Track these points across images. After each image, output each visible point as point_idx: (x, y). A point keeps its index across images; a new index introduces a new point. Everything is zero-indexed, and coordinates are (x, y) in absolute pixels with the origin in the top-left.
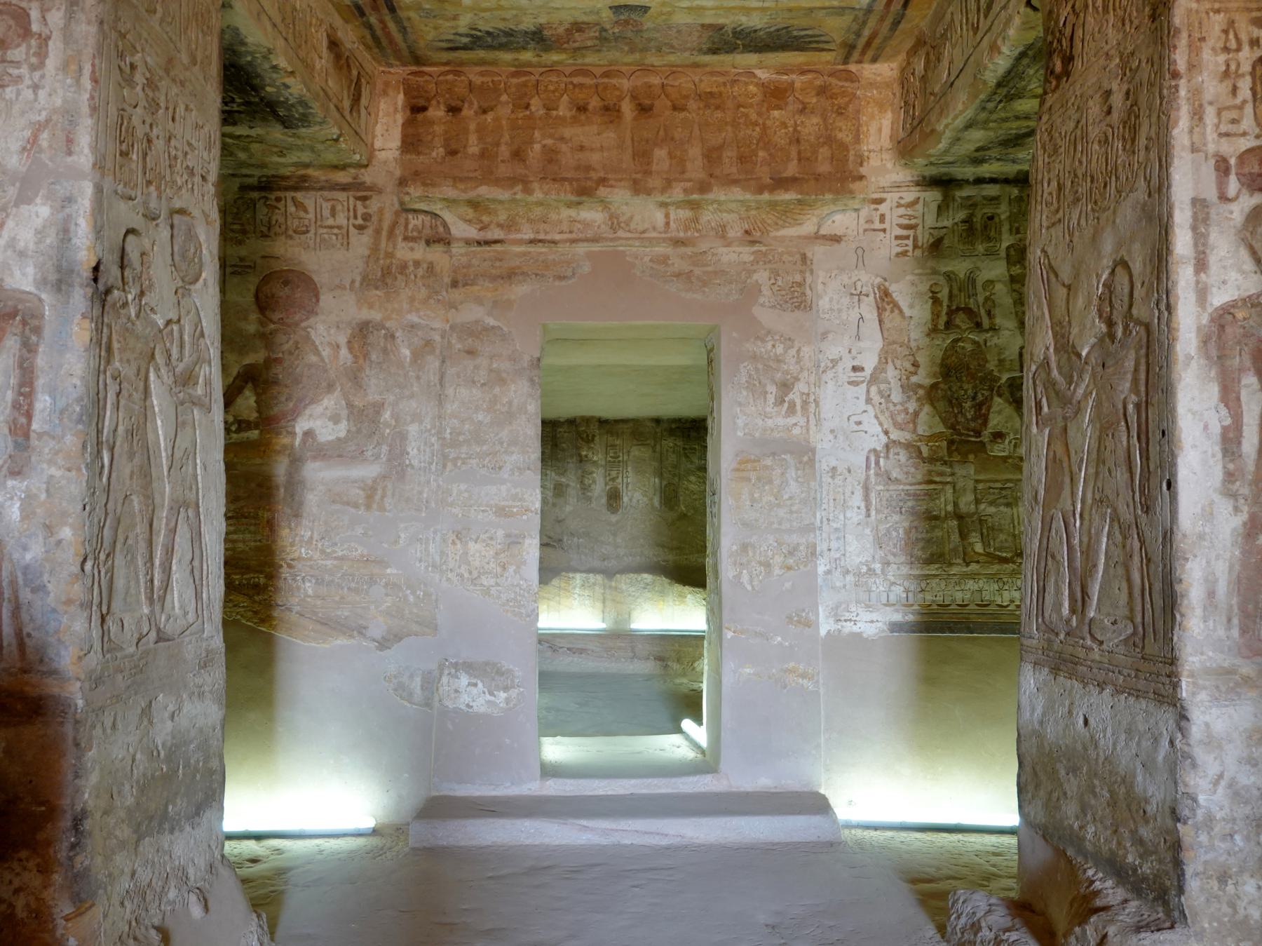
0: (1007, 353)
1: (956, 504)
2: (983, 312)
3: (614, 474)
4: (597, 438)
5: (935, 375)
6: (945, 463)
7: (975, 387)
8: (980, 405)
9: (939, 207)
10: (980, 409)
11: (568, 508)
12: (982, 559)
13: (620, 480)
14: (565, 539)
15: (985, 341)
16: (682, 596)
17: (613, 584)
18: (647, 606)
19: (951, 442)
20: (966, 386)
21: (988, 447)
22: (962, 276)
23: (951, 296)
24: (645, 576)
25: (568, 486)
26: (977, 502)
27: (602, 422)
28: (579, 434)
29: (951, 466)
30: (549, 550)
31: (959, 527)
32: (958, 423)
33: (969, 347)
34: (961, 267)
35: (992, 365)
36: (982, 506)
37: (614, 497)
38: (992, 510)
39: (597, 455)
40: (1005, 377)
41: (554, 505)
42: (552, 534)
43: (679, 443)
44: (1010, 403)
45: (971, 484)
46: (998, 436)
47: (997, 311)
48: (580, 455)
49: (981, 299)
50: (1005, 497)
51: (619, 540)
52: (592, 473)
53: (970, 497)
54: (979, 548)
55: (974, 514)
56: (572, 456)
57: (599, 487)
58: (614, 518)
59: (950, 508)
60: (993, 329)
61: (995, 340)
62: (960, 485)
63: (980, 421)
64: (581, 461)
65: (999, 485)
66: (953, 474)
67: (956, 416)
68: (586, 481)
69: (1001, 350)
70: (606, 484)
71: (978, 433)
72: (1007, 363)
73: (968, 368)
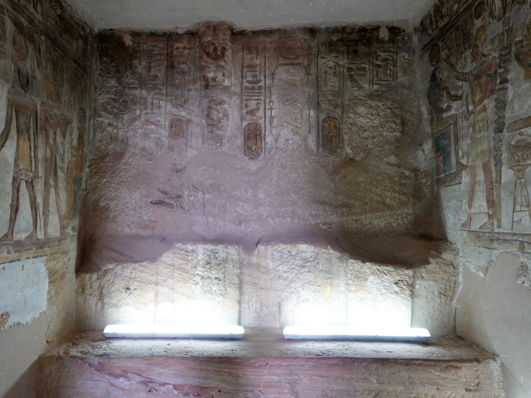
3: (252, 104)
4: (228, 53)
11: (191, 153)
13: (261, 113)
14: (186, 193)
16: (361, 278)
17: (254, 260)
18: (306, 293)
24: (303, 247)
25: (189, 121)
27: (237, 35)
28: (204, 48)
30: (163, 210)
37: (253, 136)
39: (228, 77)
41: (171, 148)
42: (167, 189)
43: (344, 61)
48: (205, 78)
51: (261, 196)
52: (222, 103)
56: (195, 81)
57: (233, 121)
58: (253, 166)
64: (207, 86)
68: (214, 114)
70: (242, 119)
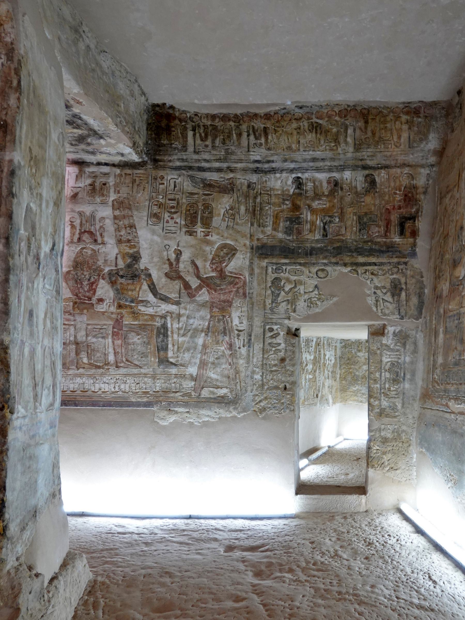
0: (109, 257)
1: (75, 337)
2: (98, 234)
5: (69, 267)
6: (71, 314)
7: (90, 274)
8: (93, 283)
9: (77, 176)
10: (92, 286)
12: (86, 366)
15: (99, 249)
19: (75, 303)
20: (85, 273)
21: (95, 306)
22: (88, 214)
23: (81, 224)
26: (87, 335)
29: (74, 316)
31: (76, 348)
32: (80, 293)
33: (90, 252)
34: (87, 209)
35: (100, 263)
36: (89, 338)
38: (94, 340)
40: (107, 269)
44: (109, 283)
45: (84, 326)
46: (101, 300)
47: (105, 234)
49: (98, 227)
50: (102, 333)
53: (83, 333)
54: (85, 360)
55: (85, 342)
59: (72, 339)
60: (103, 243)
61: (104, 249)
62: (78, 326)
63: (91, 292)
65: (99, 327)
66: (75, 320)
67: (79, 289)
69: (106, 254)
71: (90, 299)
72: (109, 262)
73: (88, 264)
